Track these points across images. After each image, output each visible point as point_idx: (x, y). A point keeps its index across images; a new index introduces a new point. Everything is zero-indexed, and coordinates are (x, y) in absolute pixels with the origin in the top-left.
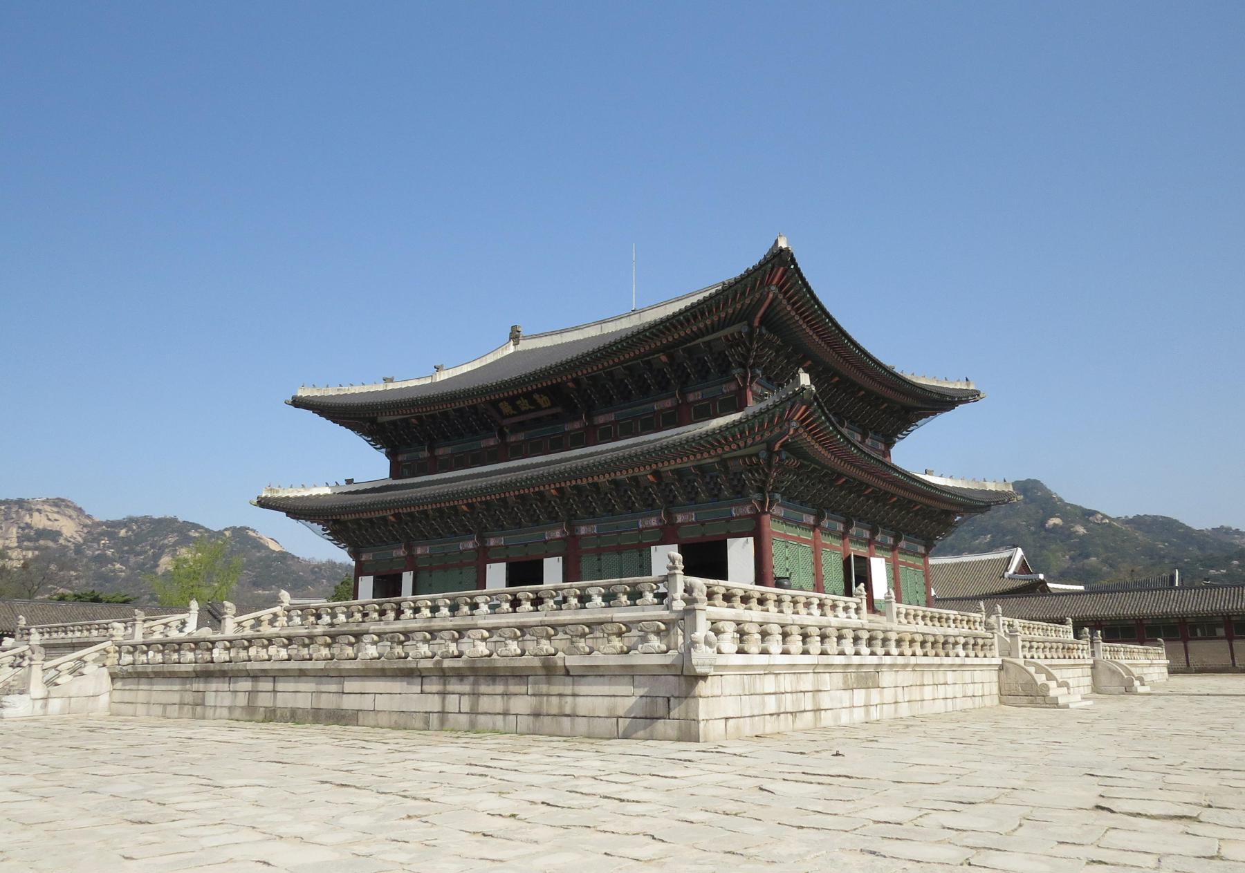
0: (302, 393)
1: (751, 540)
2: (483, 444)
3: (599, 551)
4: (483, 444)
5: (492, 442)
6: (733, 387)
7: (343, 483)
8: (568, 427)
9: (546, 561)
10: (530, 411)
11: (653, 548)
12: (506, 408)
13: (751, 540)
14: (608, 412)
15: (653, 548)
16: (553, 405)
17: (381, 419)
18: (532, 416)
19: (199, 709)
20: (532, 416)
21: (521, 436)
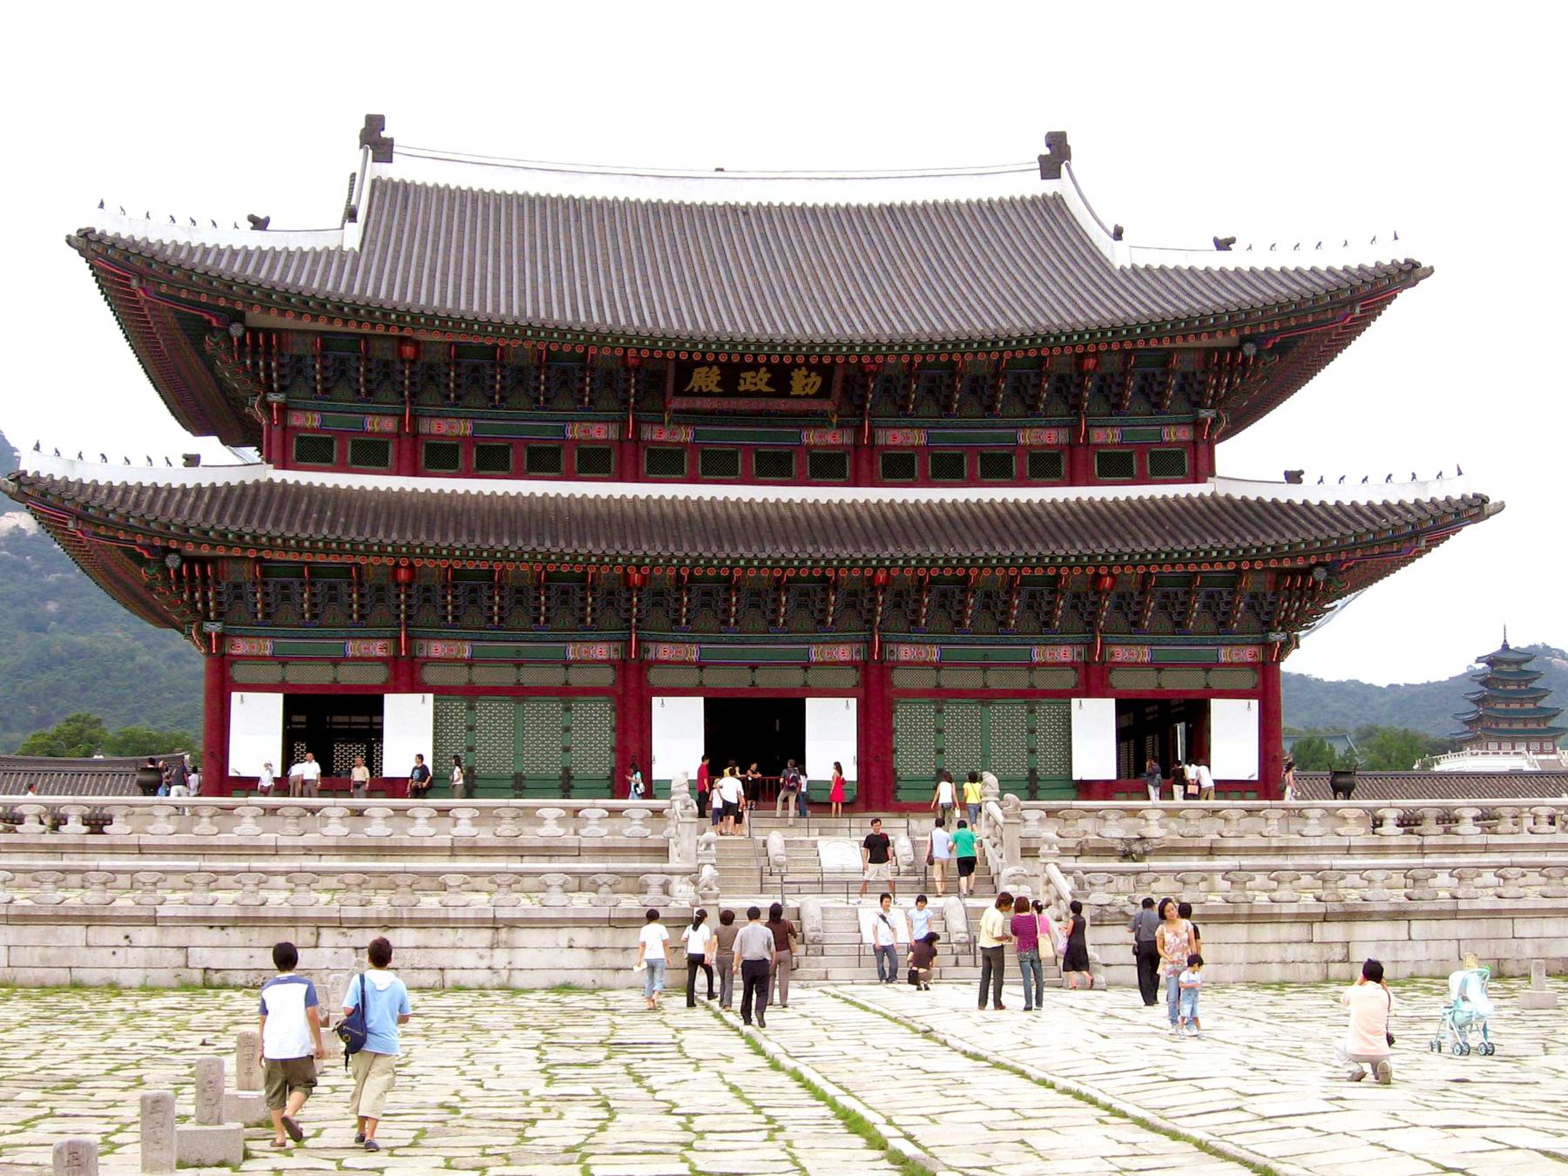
0: (109, 225)
1: (1255, 703)
2: (575, 431)
3: (940, 695)
4: (575, 431)
5: (603, 432)
6: (1185, 434)
7: (179, 462)
8: (811, 437)
9: (813, 706)
10: (759, 394)
11: (1075, 701)
12: (706, 379)
13: (1255, 703)
14: (913, 428)
15: (1075, 701)
16: (817, 396)
17: (256, 317)
18: (761, 404)
19: (1335, 970)
20: (761, 404)
21: (684, 435)
